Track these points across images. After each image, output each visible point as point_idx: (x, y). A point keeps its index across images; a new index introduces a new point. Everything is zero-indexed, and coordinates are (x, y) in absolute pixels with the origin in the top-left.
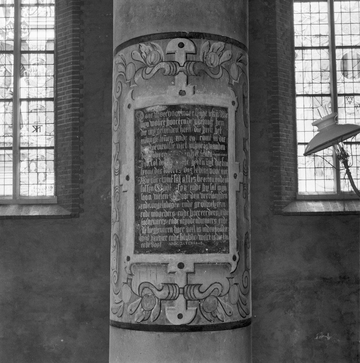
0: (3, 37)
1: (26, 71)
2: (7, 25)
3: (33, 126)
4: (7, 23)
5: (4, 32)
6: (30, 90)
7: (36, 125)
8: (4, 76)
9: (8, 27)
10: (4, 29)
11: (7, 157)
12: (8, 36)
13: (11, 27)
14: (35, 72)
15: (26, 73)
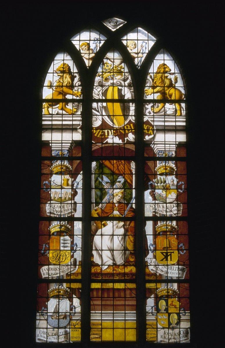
0: (121, 140)
1: (151, 182)
2: (126, 125)
3: (162, 253)
4: (126, 122)
5: (122, 133)
6: (156, 207)
7: (166, 251)
8: (122, 189)
9: (127, 127)
10: (122, 130)
11: (128, 292)
12: (127, 138)
13: (131, 127)
14: (162, 184)
15: (151, 184)
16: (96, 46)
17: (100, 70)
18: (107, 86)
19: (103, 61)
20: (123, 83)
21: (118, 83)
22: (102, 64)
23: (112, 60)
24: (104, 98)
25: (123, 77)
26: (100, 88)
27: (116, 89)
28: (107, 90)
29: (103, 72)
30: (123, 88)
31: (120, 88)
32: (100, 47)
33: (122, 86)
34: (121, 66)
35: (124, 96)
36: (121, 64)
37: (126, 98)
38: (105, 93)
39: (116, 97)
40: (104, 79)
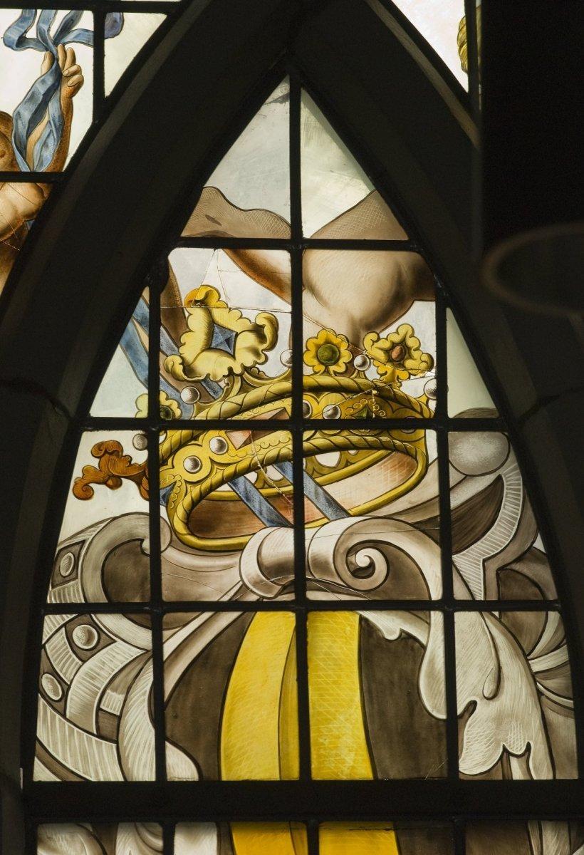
16: (58, 75)
17: (120, 391)
18: (218, 607)
19: (161, 279)
20: (427, 559)
21: (361, 559)
22: (142, 308)
23: (280, 260)
24: (181, 768)
25: (430, 487)
26: (130, 635)
27: (337, 639)
28: (218, 662)
29: (154, 423)
30: (431, 634)
31: (389, 625)
32: (102, 105)
33: (418, 607)
34: (391, 333)
35: (453, 725)
36: (395, 304)
37: (475, 759)
38: (189, 709)
39: (345, 753)
40: (175, 517)
